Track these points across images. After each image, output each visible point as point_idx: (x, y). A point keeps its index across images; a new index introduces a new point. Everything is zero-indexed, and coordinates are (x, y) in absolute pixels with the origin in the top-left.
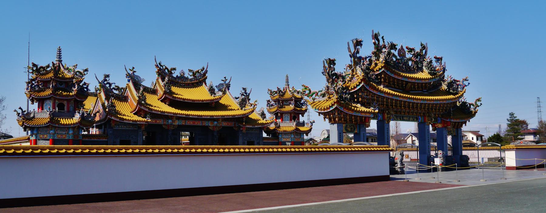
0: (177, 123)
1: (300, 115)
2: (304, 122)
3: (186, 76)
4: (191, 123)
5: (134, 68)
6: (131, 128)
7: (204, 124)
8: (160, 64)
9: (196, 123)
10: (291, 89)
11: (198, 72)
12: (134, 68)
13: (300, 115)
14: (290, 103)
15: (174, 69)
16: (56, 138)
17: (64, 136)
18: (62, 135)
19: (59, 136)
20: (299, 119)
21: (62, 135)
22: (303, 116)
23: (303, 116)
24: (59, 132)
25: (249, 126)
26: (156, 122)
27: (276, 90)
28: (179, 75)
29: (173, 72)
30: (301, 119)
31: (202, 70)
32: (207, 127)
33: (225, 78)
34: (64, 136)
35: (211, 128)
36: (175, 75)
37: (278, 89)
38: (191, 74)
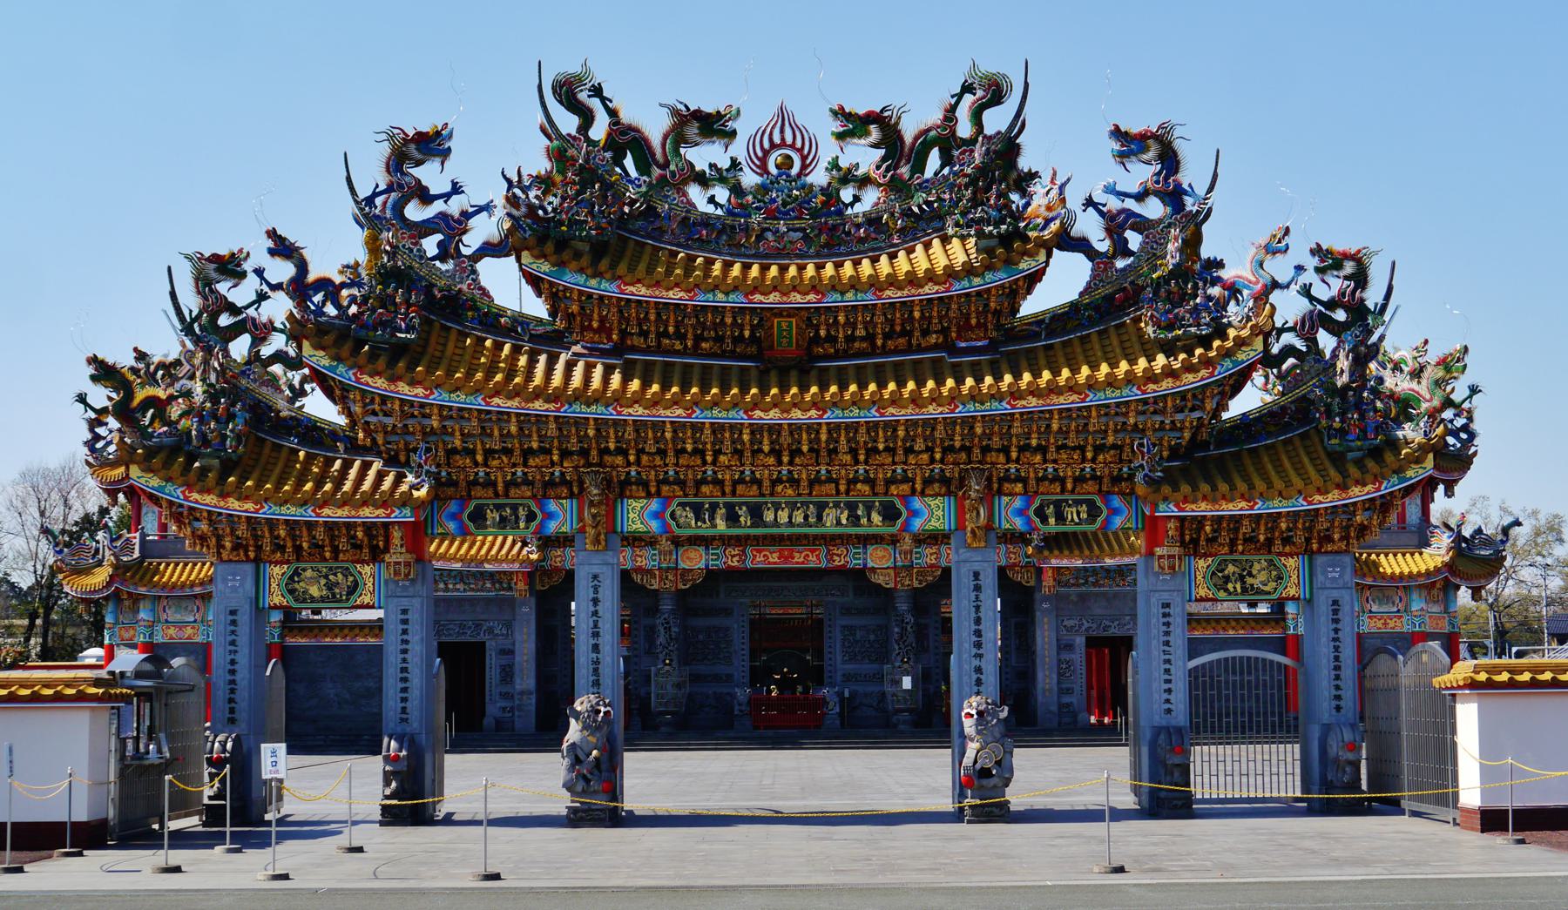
0: (696, 560)
4: (774, 558)
6: (489, 591)
7: (838, 562)
9: (798, 558)
16: (159, 638)
17: (189, 631)
18: (180, 625)
19: (172, 631)
21: (180, 625)
22: (1449, 493)
23: (1449, 493)
24: (173, 615)
25: (1065, 563)
32: (860, 576)
34: (189, 631)
35: (879, 579)
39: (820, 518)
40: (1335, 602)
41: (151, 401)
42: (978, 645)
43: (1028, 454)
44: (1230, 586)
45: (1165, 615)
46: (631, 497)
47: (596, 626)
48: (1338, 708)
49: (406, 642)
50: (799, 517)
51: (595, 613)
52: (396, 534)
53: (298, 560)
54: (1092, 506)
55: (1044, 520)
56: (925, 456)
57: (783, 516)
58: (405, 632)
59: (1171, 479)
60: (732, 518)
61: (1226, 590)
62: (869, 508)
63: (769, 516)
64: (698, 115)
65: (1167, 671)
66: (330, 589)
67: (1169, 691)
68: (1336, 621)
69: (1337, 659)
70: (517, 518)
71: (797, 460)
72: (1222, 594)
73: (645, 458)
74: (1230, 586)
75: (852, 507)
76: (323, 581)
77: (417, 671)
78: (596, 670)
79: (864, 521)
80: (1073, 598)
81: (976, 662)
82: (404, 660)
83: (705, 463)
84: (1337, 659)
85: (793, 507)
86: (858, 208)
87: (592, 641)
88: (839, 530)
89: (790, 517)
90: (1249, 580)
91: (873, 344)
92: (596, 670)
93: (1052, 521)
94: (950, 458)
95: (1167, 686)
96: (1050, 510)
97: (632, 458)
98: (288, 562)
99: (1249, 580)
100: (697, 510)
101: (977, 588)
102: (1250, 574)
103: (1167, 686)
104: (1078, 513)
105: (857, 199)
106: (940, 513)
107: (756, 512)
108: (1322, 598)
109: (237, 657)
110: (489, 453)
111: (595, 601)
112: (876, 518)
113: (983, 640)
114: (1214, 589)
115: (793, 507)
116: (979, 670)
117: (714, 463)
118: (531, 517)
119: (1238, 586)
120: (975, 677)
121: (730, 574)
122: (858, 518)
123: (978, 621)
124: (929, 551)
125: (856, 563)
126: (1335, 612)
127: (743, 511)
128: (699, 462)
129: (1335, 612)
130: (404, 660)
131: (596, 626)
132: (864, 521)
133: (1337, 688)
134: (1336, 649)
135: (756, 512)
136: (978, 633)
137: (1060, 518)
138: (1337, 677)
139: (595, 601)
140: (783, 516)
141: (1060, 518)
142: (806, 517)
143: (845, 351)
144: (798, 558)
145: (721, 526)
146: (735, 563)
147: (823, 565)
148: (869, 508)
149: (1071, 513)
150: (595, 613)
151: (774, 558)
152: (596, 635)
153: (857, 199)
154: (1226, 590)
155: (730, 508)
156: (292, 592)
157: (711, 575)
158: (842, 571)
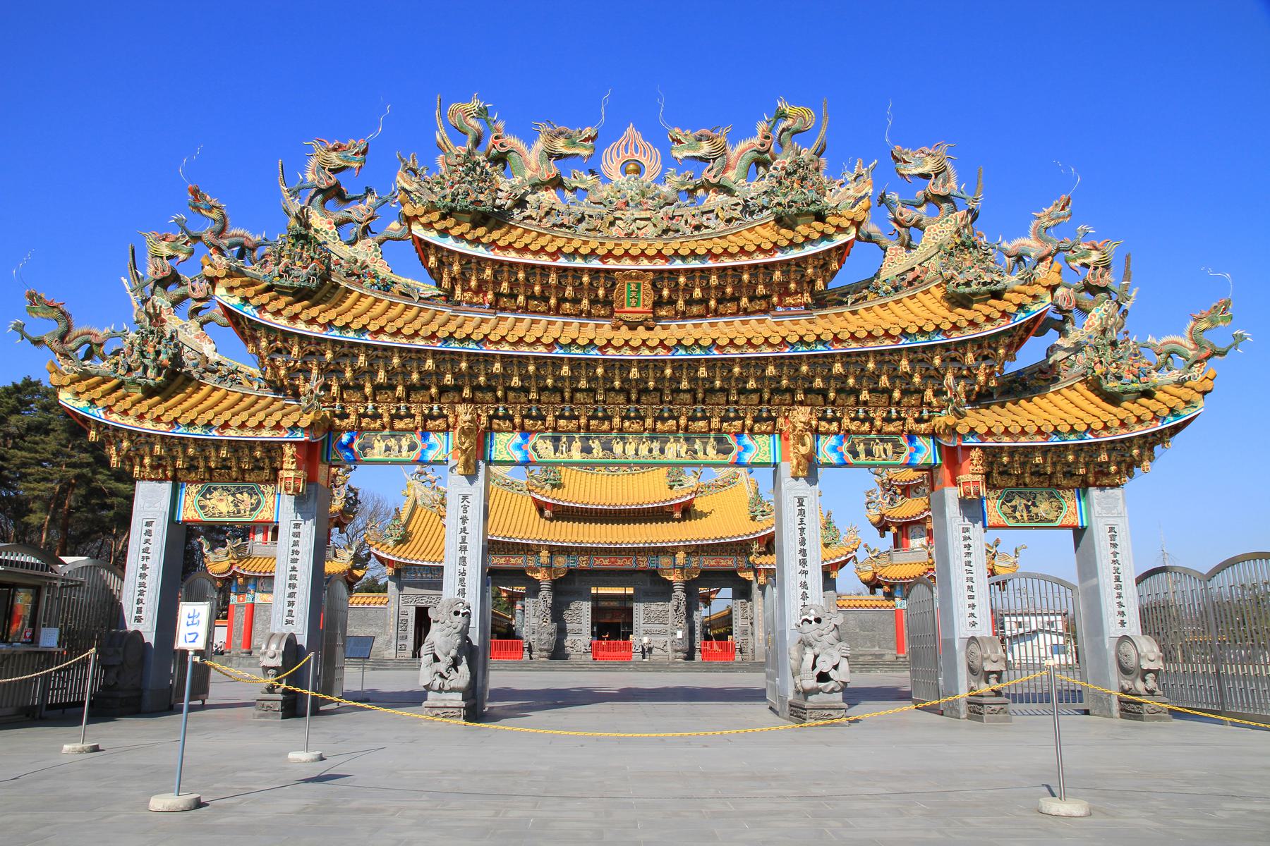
0: (562, 562)
7: (642, 565)
39: (662, 451)
40: (1112, 529)
42: (803, 563)
43: (843, 396)
44: (1018, 514)
45: (966, 539)
46: (499, 431)
47: (463, 541)
48: (1123, 623)
49: (297, 552)
50: (644, 450)
51: (464, 530)
52: (289, 451)
53: (211, 480)
54: (896, 445)
55: (855, 454)
56: (755, 397)
58: (296, 543)
61: (1015, 518)
63: (618, 448)
65: (970, 588)
66: (236, 506)
67: (973, 606)
68: (1115, 546)
69: (1118, 579)
70: (400, 447)
71: (643, 398)
72: (1011, 523)
73: (511, 395)
74: (1018, 514)
76: (231, 498)
77: (304, 577)
78: (462, 581)
79: (700, 454)
81: (802, 578)
82: (294, 569)
83: (563, 400)
84: (1118, 579)
87: (460, 554)
88: (679, 460)
89: (637, 450)
90: (1033, 509)
91: (707, 307)
92: (462, 581)
93: (862, 456)
94: (777, 398)
95: (971, 601)
96: (861, 448)
97: (499, 393)
98: (202, 481)
99: (1033, 509)
100: (556, 440)
101: (802, 512)
102: (1034, 504)
103: (971, 601)
104: (885, 450)
106: (766, 448)
108: (1101, 525)
109: (148, 563)
110: (377, 388)
111: (464, 520)
112: (711, 452)
113: (808, 558)
114: (1004, 518)
116: (804, 585)
117: (572, 400)
119: (1025, 514)
120: (801, 591)
121: (582, 572)
122: (695, 452)
123: (803, 542)
125: (653, 566)
126: (1113, 537)
127: (596, 445)
128: (558, 399)
129: (1113, 537)
130: (294, 569)
131: (463, 541)
132: (700, 454)
133: (1120, 605)
134: (1117, 570)
135: (607, 448)
136: (803, 552)
137: (869, 453)
138: (1119, 596)
139: (464, 520)
140: (630, 449)
142: (650, 451)
143: (684, 313)
144: (620, 562)
145: (576, 455)
146: (584, 565)
150: (464, 530)
151: (606, 562)
152: (464, 549)
154: (1015, 518)
156: (203, 507)
157: (571, 572)
158: (643, 571)
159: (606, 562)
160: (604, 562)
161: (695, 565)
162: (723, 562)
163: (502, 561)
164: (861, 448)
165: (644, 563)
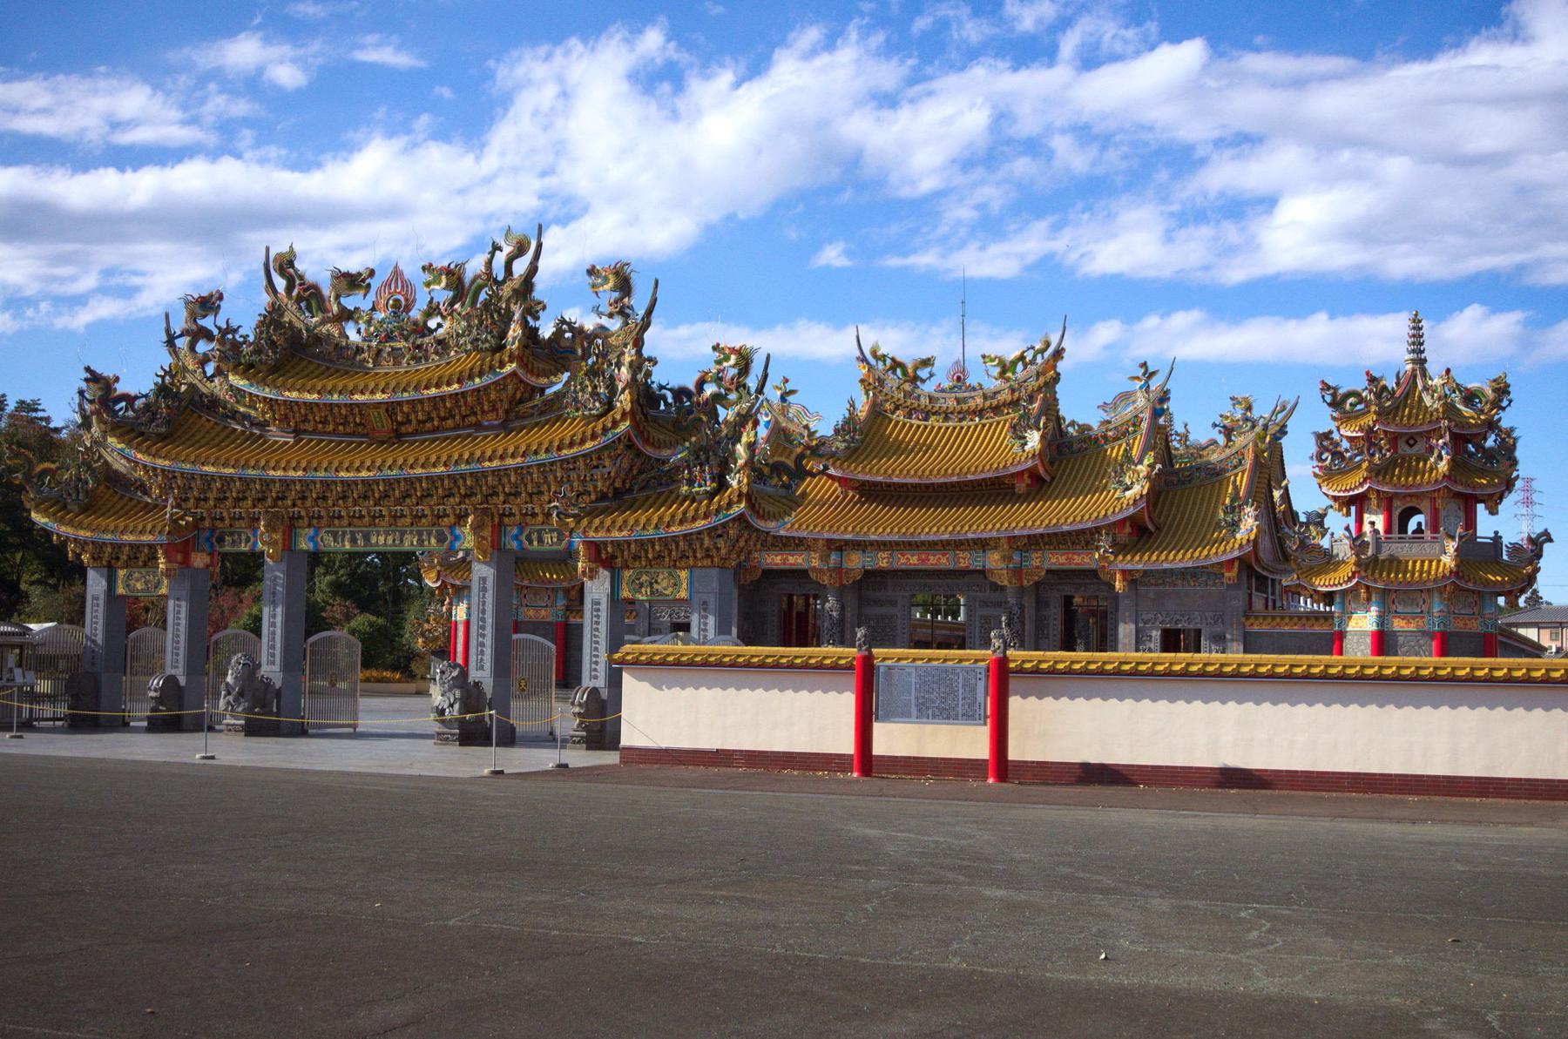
0: (856, 562)
1: (1481, 507)
2: (1497, 538)
3: (971, 381)
5: (786, 381)
8: (874, 353)
10: (1437, 381)
11: (1022, 358)
12: (786, 381)
13: (1481, 507)
14: (1431, 450)
15: (927, 363)
20: (1471, 523)
22: (1493, 511)
23: (1493, 511)
26: (784, 561)
27: (1360, 384)
28: (946, 384)
29: (923, 373)
30: (1486, 524)
31: (1042, 351)
33: (1144, 365)
36: (928, 388)
37: (1373, 380)
38: (996, 371)
41: (45, 472)
50: (390, 542)
57: (382, 539)
59: (592, 513)
60: (353, 541)
62: (429, 535)
63: (374, 540)
64: (346, 275)
75: (420, 534)
80: (1151, 595)
85: (387, 534)
86: (441, 331)
100: (335, 535)
105: (440, 326)
107: (367, 537)
112: (433, 541)
115: (387, 534)
118: (248, 540)
124: (1034, 555)
125: (978, 565)
127: (359, 536)
140: (382, 539)
141: (540, 541)
144: (933, 560)
145: (348, 546)
146: (884, 564)
147: (951, 567)
148: (429, 535)
149: (547, 538)
151: (914, 560)
153: (440, 326)
155: (353, 533)
157: (869, 574)
159: (914, 560)
160: (912, 560)
161: (1036, 563)
162: (1077, 559)
163: (778, 559)
164: (534, 536)
165: (965, 560)
